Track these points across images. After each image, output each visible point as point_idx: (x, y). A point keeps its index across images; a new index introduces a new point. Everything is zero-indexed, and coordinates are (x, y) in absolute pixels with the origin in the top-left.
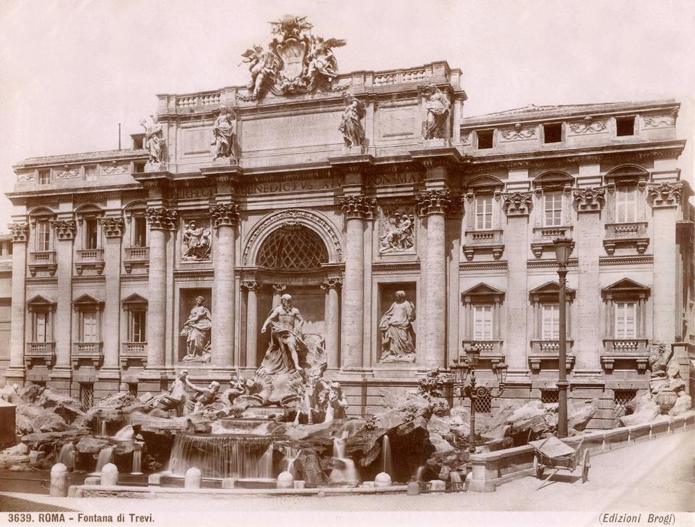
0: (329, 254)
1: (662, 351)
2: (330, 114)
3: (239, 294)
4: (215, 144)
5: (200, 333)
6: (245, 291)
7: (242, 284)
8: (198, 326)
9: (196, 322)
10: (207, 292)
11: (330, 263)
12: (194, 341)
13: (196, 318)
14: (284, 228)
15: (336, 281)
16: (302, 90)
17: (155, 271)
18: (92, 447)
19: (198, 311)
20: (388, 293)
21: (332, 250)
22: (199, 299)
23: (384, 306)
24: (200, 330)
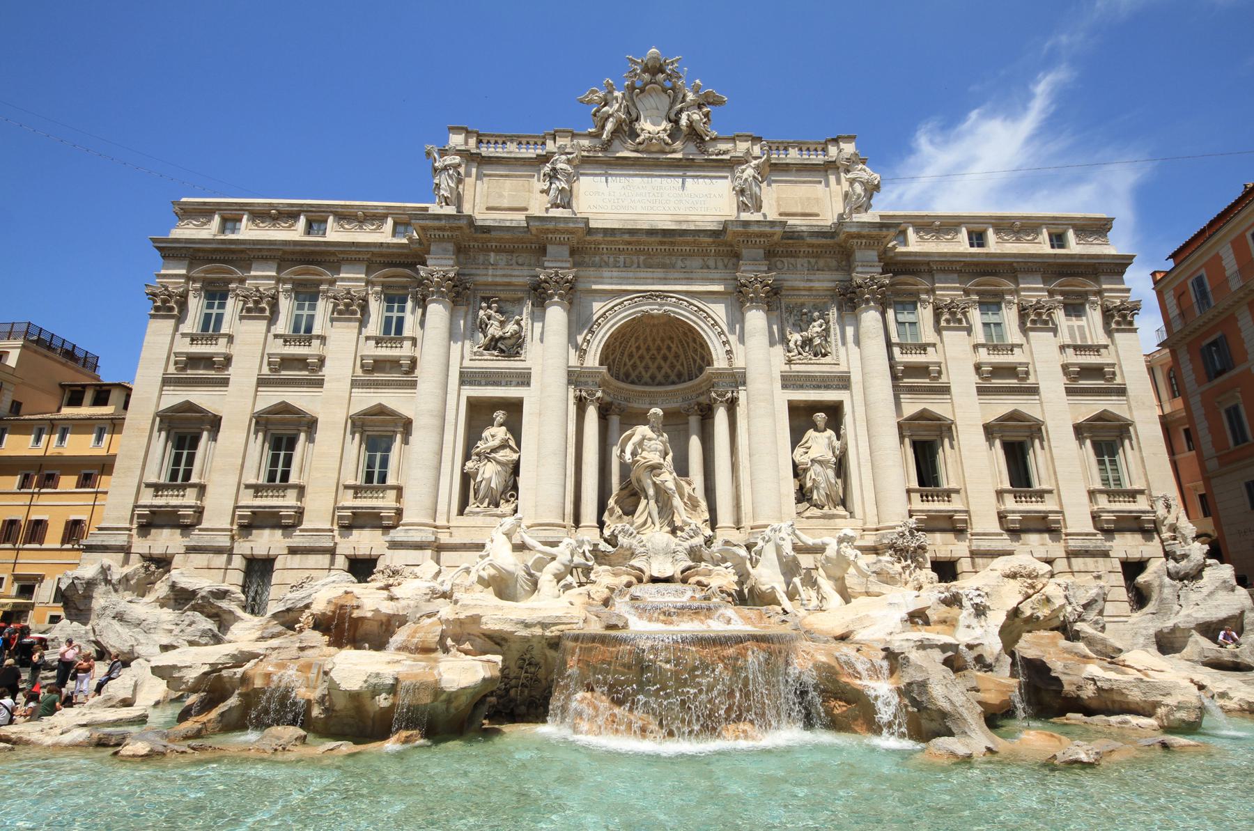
0: (714, 357)
1: (1168, 507)
2: (707, 181)
3: (572, 409)
4: (546, 192)
5: (499, 468)
6: (581, 404)
7: (578, 393)
8: (500, 455)
9: (494, 450)
10: (514, 408)
11: (716, 365)
12: (490, 480)
13: (496, 443)
14: (648, 316)
15: (729, 395)
16: (667, 149)
17: (427, 374)
18: (378, 675)
19: (496, 434)
20: (802, 418)
21: (719, 351)
22: (500, 416)
23: (797, 437)
24: (498, 462)
